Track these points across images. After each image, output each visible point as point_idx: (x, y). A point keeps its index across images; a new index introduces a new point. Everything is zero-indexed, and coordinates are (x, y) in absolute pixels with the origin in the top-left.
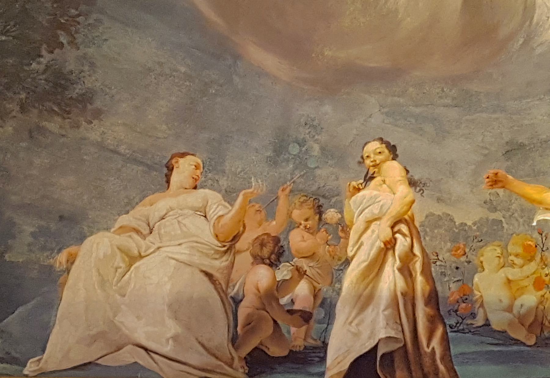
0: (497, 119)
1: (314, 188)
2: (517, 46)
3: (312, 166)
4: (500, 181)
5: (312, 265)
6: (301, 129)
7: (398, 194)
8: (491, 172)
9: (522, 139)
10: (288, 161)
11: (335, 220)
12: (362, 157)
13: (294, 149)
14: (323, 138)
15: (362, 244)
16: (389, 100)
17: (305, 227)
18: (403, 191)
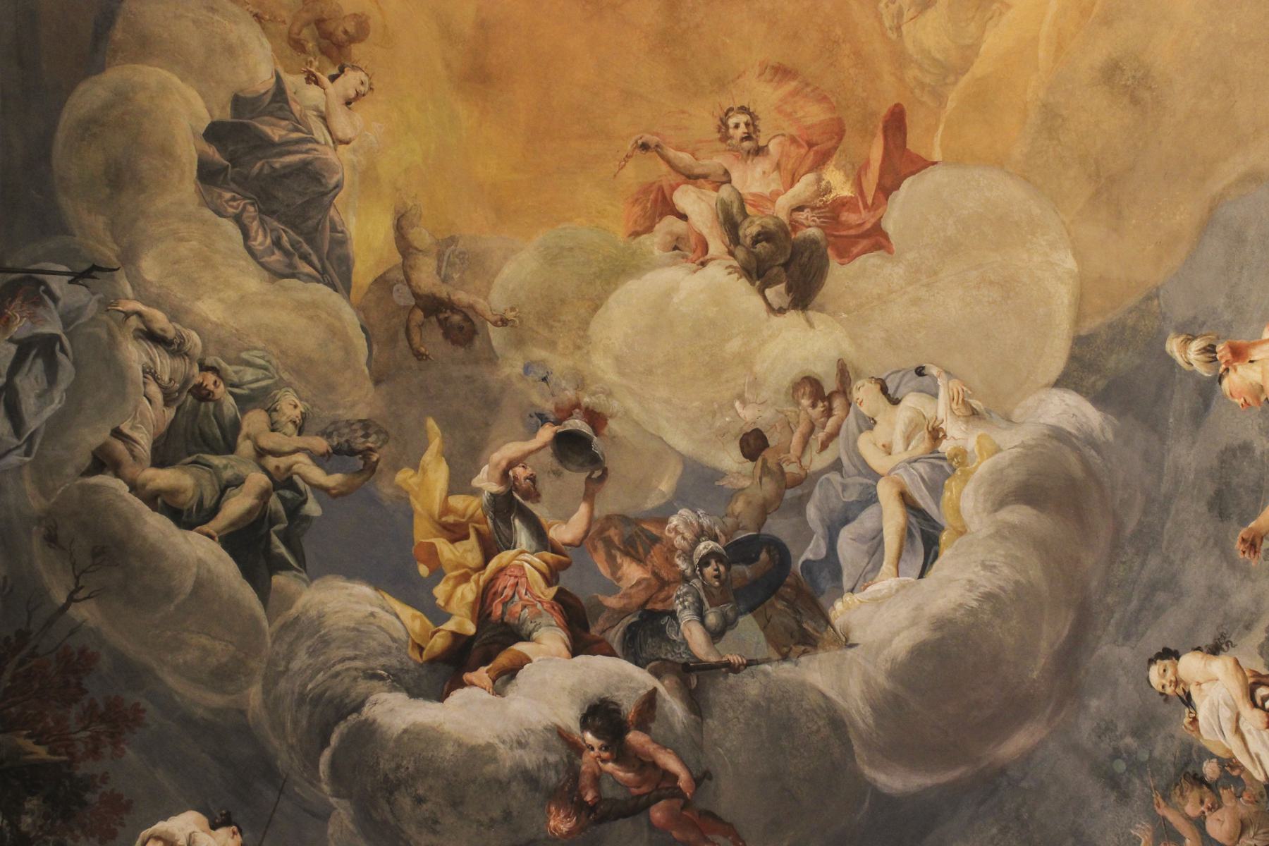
0: (1177, 510)
1: (1172, 770)
2: (1098, 461)
3: (1147, 757)
4: (1253, 539)
5: (1252, 833)
6: (1103, 745)
7: (1220, 675)
8: (1238, 546)
9: (1210, 489)
10: (1129, 781)
11: (1217, 770)
12: (1162, 694)
13: (1120, 766)
14: (1121, 726)
15: (1258, 756)
16: (1111, 629)
17: (1209, 809)
18: (1220, 666)
